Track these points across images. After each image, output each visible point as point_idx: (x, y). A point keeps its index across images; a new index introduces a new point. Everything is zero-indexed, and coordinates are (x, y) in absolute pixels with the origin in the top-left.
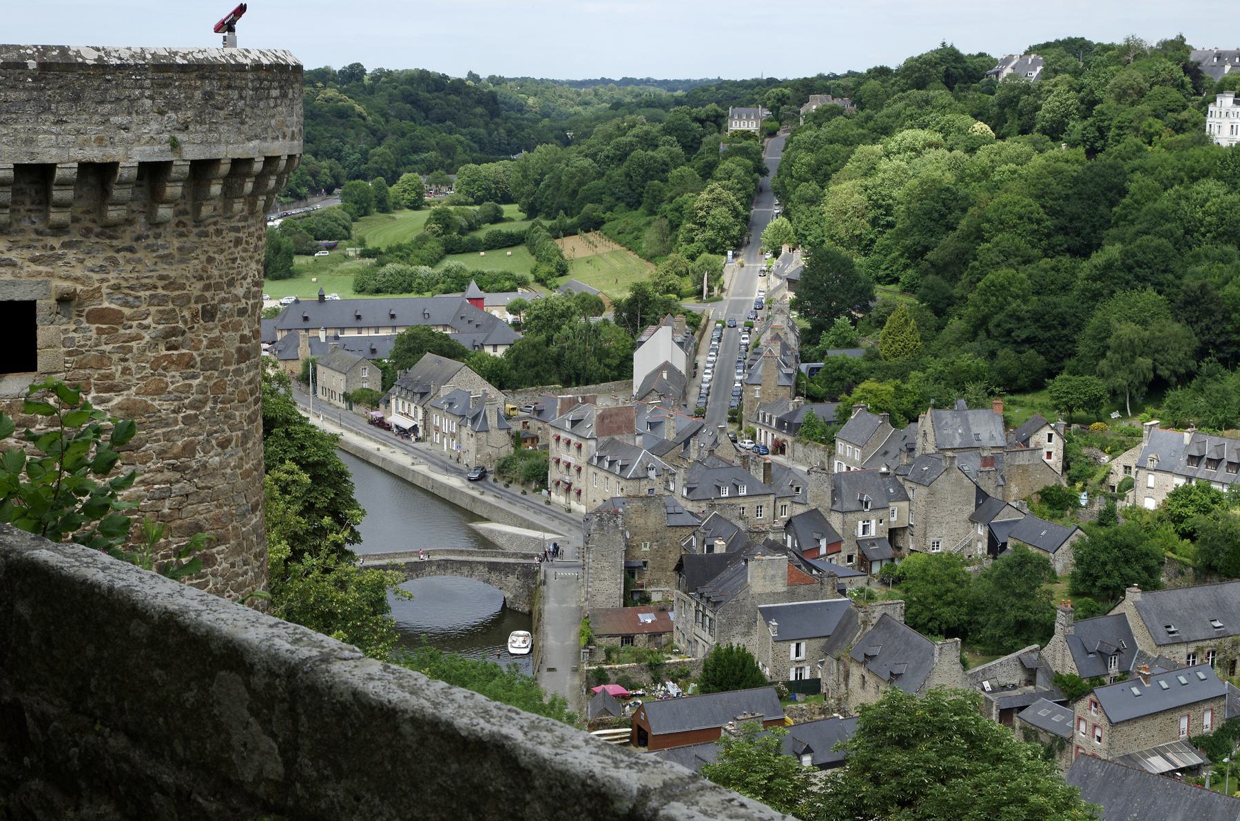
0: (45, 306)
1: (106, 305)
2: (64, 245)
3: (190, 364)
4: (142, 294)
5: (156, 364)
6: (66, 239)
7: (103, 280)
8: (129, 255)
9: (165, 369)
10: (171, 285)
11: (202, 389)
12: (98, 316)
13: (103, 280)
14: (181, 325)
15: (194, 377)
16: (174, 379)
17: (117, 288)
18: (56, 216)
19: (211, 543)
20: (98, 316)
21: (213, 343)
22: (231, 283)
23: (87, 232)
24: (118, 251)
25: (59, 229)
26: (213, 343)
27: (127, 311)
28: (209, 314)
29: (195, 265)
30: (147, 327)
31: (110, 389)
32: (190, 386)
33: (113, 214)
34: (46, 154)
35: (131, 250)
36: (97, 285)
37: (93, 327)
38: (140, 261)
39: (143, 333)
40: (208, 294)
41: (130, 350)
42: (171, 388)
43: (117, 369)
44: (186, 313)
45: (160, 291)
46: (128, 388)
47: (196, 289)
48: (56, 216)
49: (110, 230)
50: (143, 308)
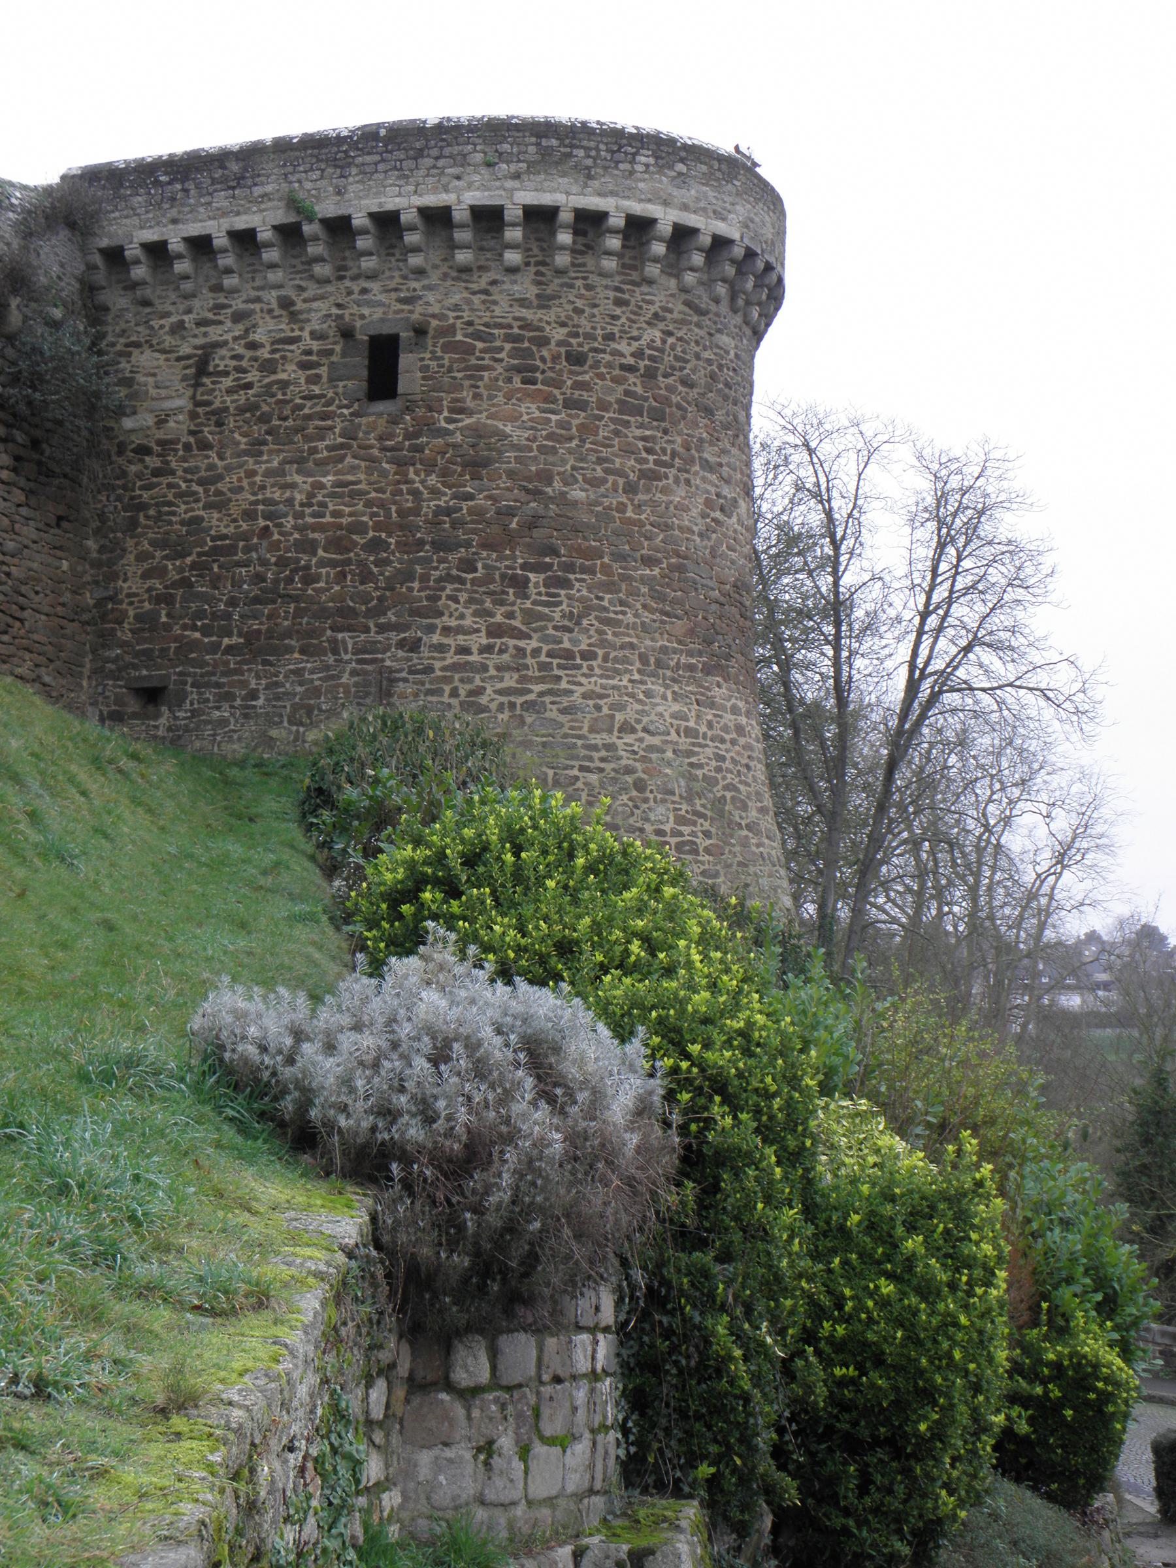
1: (459, 337)
2: (424, 288)
4: (496, 331)
6: (426, 282)
7: (457, 318)
8: (483, 297)
9: (519, 400)
10: (526, 326)
13: (457, 318)
14: (538, 363)
15: (553, 412)
17: (470, 323)
18: (415, 260)
19: (569, 568)
20: (449, 347)
21: (578, 385)
22: (610, 337)
23: (445, 276)
24: (474, 293)
26: (578, 385)
27: (480, 345)
28: (577, 359)
30: (501, 360)
31: (461, 411)
32: (549, 420)
33: (463, 257)
35: (486, 292)
36: (451, 321)
37: (447, 356)
38: (495, 303)
39: (496, 365)
40: (573, 341)
41: (481, 378)
42: (525, 418)
43: (466, 394)
44: (545, 353)
45: (516, 330)
46: (480, 412)
47: (559, 334)
48: (415, 260)
50: (498, 344)
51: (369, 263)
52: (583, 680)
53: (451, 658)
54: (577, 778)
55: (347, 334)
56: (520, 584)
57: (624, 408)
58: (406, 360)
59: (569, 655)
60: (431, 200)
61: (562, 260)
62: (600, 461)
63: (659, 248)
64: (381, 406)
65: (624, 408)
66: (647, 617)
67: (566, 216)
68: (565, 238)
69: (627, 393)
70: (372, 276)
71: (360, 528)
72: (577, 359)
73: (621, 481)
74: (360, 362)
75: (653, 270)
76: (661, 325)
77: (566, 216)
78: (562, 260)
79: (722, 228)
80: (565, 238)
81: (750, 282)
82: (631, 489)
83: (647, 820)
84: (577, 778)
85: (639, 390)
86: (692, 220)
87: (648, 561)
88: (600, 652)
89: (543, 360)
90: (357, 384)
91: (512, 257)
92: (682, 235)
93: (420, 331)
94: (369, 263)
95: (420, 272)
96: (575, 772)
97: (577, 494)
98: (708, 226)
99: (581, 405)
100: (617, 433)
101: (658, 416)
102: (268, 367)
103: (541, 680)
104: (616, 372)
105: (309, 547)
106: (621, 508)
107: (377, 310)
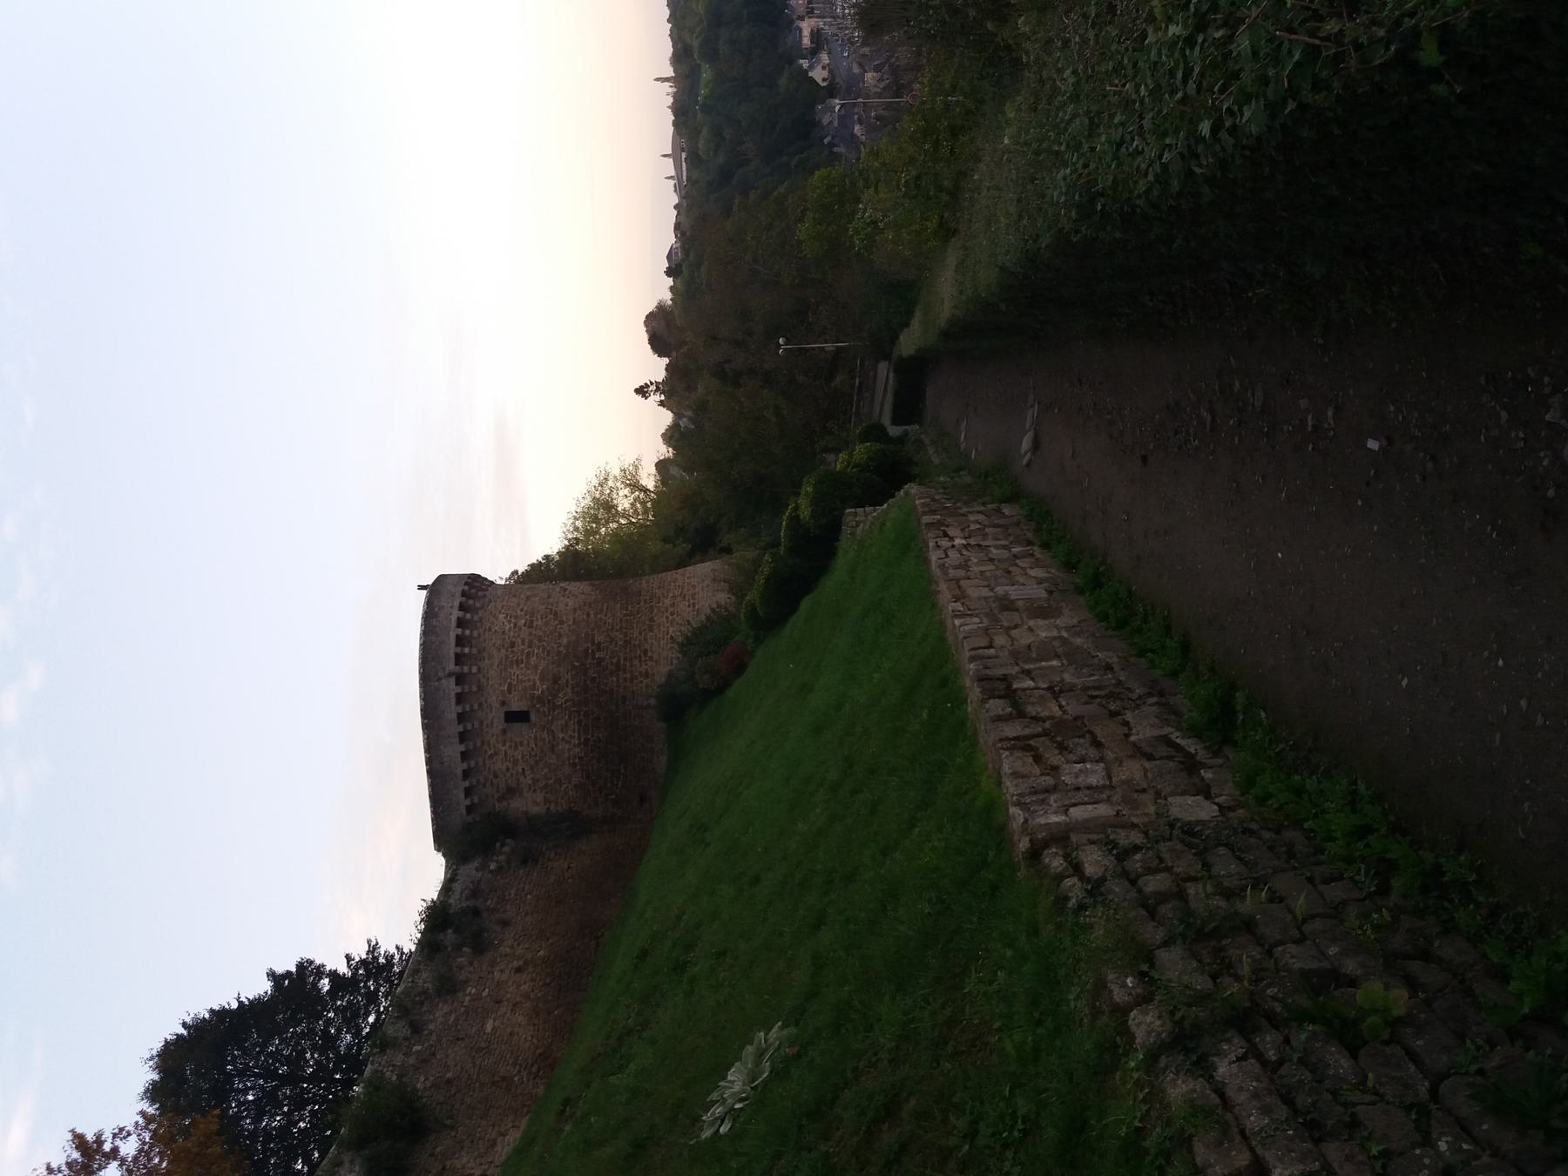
0: (505, 709)
10: (500, 663)
12: (509, 691)
16: (533, 660)
20: (509, 691)
25: (480, 705)
28: (513, 645)
29: (495, 652)
33: (474, 688)
34: (454, 716)
49: (480, 688)
51: (477, 725)
55: (504, 731)
56: (600, 660)
57: (531, 626)
58: (516, 706)
60: (453, 701)
61: (474, 651)
63: (468, 616)
64: (533, 717)
65: (531, 626)
67: (459, 650)
68: (467, 650)
70: (481, 723)
71: (579, 722)
72: (513, 645)
74: (517, 725)
75: (476, 618)
77: (459, 650)
78: (474, 651)
79: (459, 594)
80: (467, 650)
81: (474, 584)
82: (562, 623)
86: (456, 604)
90: (524, 727)
91: (474, 670)
92: (462, 607)
93: (503, 703)
94: (477, 725)
95: (480, 705)
97: (565, 641)
99: (531, 642)
101: (532, 614)
102: (516, 763)
105: (587, 740)
107: (495, 717)
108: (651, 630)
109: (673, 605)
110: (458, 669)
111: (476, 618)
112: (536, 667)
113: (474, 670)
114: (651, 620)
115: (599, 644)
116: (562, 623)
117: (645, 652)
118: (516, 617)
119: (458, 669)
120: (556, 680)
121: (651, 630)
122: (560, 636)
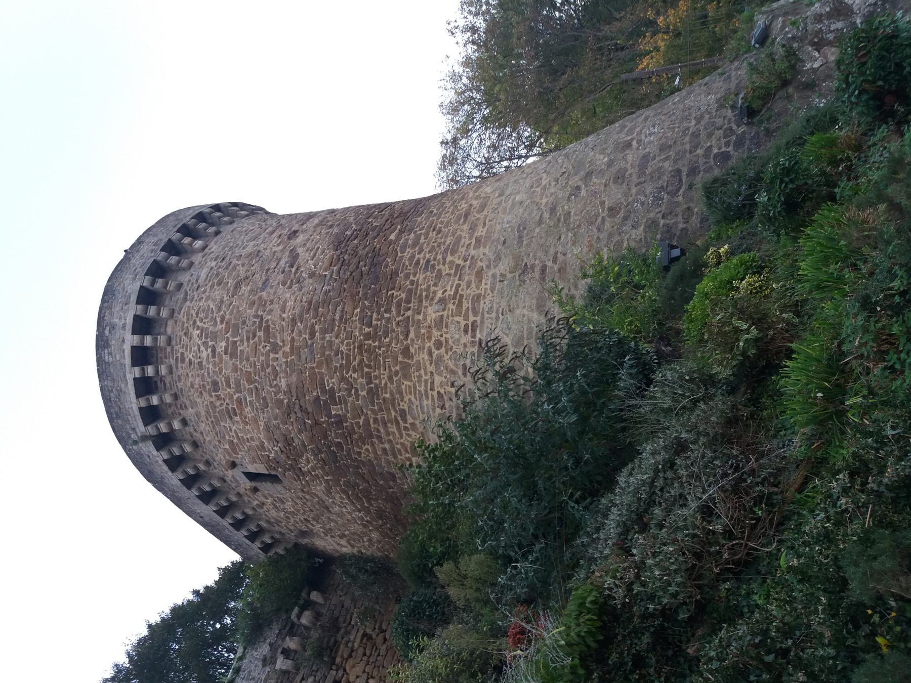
3: (239, 401)
5: (246, 423)
11: (250, 392)
14: (224, 407)
15: (246, 399)
28: (215, 385)
40: (208, 387)
49: (195, 445)
52: (383, 382)
53: (391, 458)
54: (439, 393)
59: (370, 391)
62: (263, 369)
65: (233, 355)
66: (343, 335)
67: (143, 404)
69: (226, 353)
73: (272, 355)
76: (191, 329)
83: (458, 340)
84: (439, 393)
85: (223, 344)
87: (312, 334)
88: (366, 370)
89: (221, 405)
96: (435, 393)
97: (283, 383)
98: (134, 309)
99: (238, 384)
100: (248, 360)
103: (388, 410)
104: (217, 359)
106: (285, 355)
108: (407, 376)
109: (440, 323)
110: (151, 430)
111: (162, 340)
112: (256, 420)
113: (176, 425)
114: (406, 352)
115: (332, 392)
116: (275, 348)
117: (403, 414)
118: (215, 336)
119: (151, 430)
120: (288, 441)
121: (407, 376)
122: (276, 374)
